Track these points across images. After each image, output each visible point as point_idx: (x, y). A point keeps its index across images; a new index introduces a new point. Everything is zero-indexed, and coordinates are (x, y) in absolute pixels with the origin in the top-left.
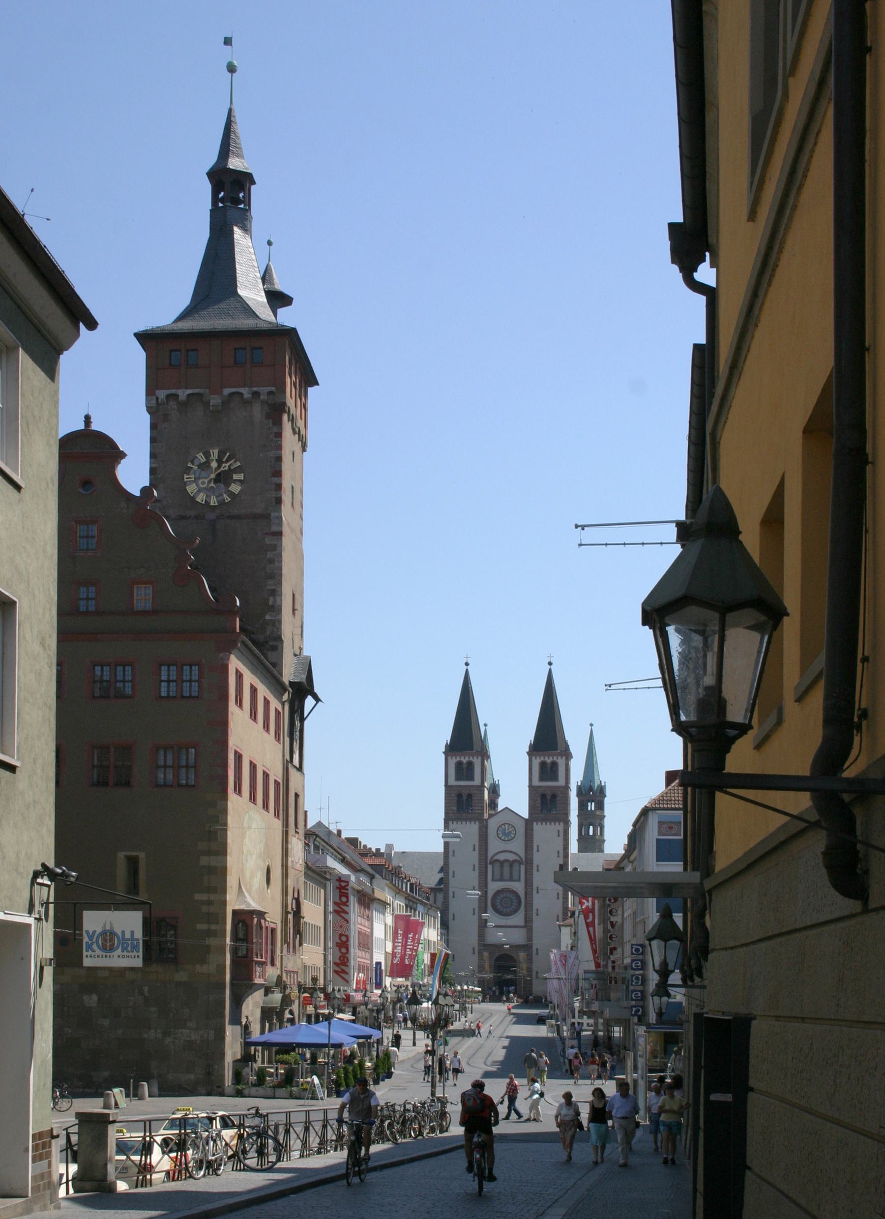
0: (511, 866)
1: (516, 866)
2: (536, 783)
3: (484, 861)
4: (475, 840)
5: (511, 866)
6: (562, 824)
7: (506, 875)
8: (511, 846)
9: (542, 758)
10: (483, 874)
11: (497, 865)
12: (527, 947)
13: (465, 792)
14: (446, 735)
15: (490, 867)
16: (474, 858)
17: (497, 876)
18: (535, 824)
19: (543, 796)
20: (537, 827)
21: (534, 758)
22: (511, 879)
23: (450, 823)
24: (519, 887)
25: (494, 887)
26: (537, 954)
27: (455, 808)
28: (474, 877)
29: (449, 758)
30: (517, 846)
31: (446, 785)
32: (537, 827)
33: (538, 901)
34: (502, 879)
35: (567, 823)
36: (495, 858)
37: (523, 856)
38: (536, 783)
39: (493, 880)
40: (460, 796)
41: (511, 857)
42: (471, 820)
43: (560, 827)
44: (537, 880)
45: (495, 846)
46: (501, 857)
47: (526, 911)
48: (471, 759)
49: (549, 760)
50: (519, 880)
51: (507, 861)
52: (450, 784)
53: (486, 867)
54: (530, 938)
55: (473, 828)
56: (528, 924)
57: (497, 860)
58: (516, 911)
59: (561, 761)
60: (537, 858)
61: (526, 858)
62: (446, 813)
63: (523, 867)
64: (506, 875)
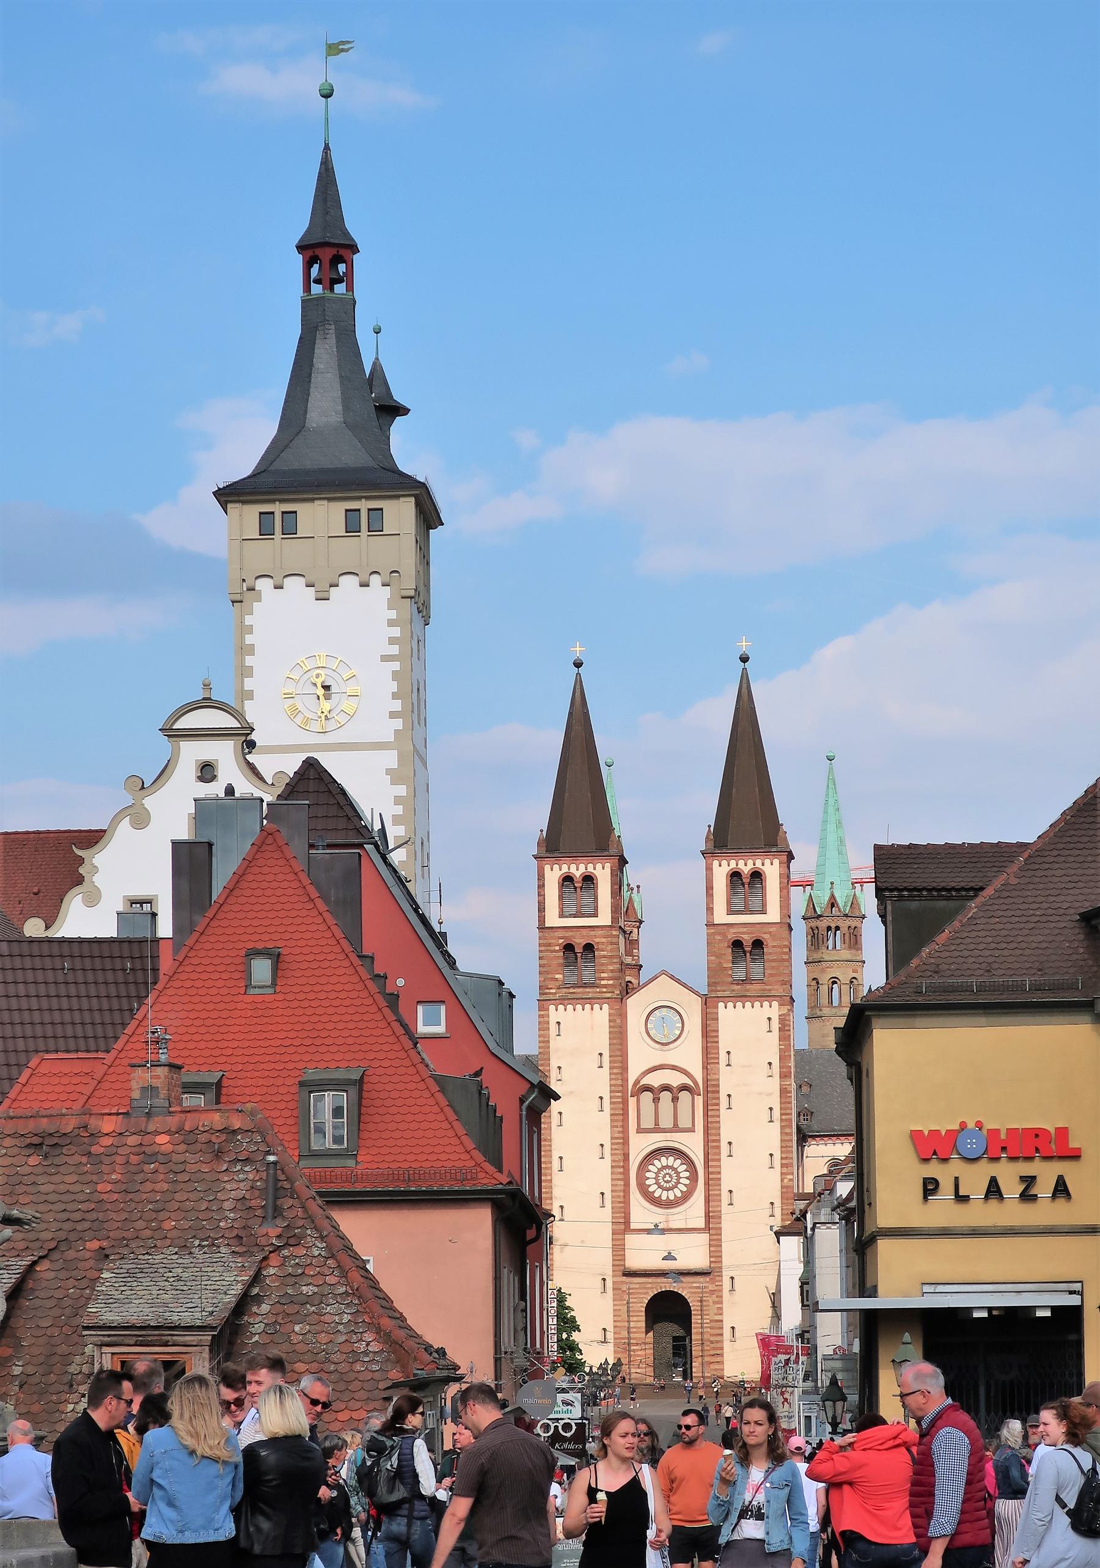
0: (675, 1099)
3: (624, 1093)
4: (602, 1041)
5: (675, 1099)
6: (775, 1004)
7: (666, 1122)
8: (671, 1056)
9: (733, 864)
10: (620, 1117)
13: (579, 941)
14: (537, 816)
15: (632, 1101)
16: (601, 1082)
17: (648, 1122)
18: (721, 1005)
20: (729, 1015)
21: (716, 863)
22: (676, 1128)
23: (552, 1008)
24: (693, 1144)
25: (640, 1145)
26: (732, 1290)
29: (547, 868)
30: (688, 1055)
31: (542, 927)
32: (729, 1015)
33: (730, 1174)
34: (657, 1129)
36: (645, 1081)
37: (699, 1076)
38: (721, 916)
39: (640, 1130)
40: (569, 948)
41: (675, 1079)
42: (591, 1001)
43: (773, 1010)
45: (641, 1056)
46: (655, 1080)
47: (707, 1200)
48: (590, 868)
49: (746, 867)
50: (692, 1130)
51: (666, 1088)
55: (601, 1015)
56: (712, 1223)
57: (648, 1088)
58: (686, 1196)
59: (772, 869)
60: (727, 1081)
61: (706, 1081)
63: (699, 1101)
64: (666, 1122)
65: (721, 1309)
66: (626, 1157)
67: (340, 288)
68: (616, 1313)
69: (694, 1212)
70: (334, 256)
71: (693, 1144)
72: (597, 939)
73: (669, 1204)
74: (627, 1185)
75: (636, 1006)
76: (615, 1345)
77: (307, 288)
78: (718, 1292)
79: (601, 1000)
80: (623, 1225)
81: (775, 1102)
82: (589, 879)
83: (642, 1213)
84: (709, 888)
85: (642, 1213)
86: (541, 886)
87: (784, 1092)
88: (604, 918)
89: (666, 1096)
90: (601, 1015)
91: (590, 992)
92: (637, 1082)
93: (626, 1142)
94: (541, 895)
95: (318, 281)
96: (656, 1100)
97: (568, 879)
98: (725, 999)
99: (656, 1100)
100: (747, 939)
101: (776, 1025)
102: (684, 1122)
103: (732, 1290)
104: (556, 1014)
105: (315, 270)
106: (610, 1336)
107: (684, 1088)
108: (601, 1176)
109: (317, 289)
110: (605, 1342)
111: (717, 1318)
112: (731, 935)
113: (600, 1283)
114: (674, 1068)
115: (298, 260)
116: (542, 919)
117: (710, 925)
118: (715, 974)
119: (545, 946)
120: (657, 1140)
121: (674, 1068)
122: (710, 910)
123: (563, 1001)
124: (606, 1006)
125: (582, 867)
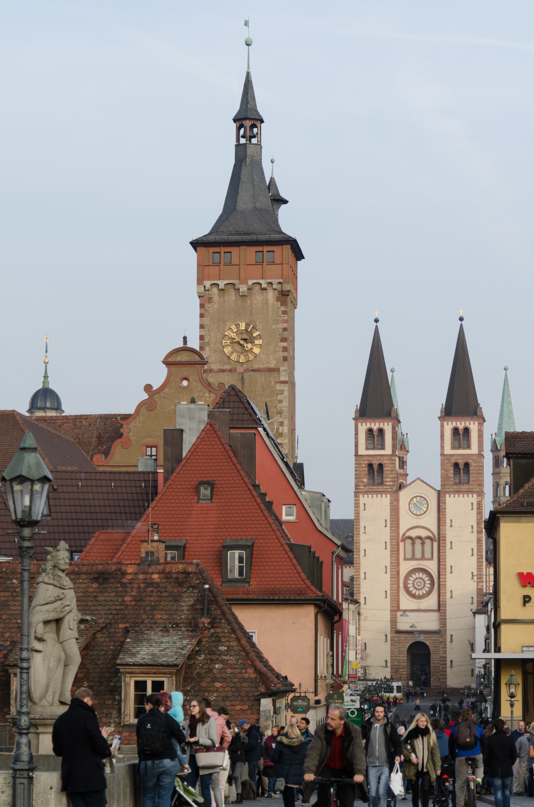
0: (423, 543)
1: (428, 542)
2: (448, 450)
3: (397, 540)
6: (475, 495)
7: (418, 555)
8: (422, 521)
11: (409, 542)
12: (440, 633)
13: (375, 462)
15: (401, 544)
16: (386, 534)
17: (409, 555)
18: (447, 496)
19: (456, 465)
20: (450, 500)
21: (445, 423)
22: (423, 558)
23: (361, 496)
24: (432, 566)
25: (405, 567)
26: (451, 641)
27: (365, 480)
28: (385, 558)
29: (359, 424)
30: (430, 521)
31: (356, 455)
32: (450, 500)
34: (413, 558)
35: (481, 494)
36: (408, 534)
38: (448, 450)
39: (405, 559)
40: (370, 466)
41: (424, 533)
42: (381, 493)
43: (474, 499)
44: (450, 559)
45: (406, 521)
46: (413, 533)
50: (432, 559)
51: (420, 538)
52: (360, 453)
53: (398, 545)
54: (443, 620)
55: (385, 500)
56: (441, 608)
57: (410, 538)
58: (429, 593)
59: (474, 427)
60: (450, 534)
61: (439, 534)
62: (356, 486)
63: (435, 544)
64: (418, 555)
65: (446, 651)
66: (398, 573)
67: (254, 141)
68: (392, 653)
69: (431, 601)
70: (252, 124)
71: (432, 566)
72: (385, 462)
73: (420, 597)
74: (398, 587)
75: (404, 496)
76: (392, 669)
77: (238, 140)
78: (444, 643)
79: (386, 492)
80: (395, 608)
81: (475, 546)
82: (381, 431)
83: (406, 602)
84: (442, 436)
85: (406, 602)
86: (356, 434)
87: (479, 541)
88: (388, 450)
89: (418, 542)
90: (385, 500)
91: (381, 488)
92: (404, 534)
93: (398, 565)
94: (356, 438)
95: (243, 137)
96: (413, 544)
97: (370, 430)
98: (449, 493)
99: (413, 544)
100: (461, 462)
101: (475, 507)
102: (428, 555)
103: (451, 641)
104: (363, 499)
105: (242, 131)
106: (389, 664)
107: (429, 538)
108: (385, 582)
109: (243, 141)
110: (386, 667)
111: (444, 655)
112: (453, 460)
113: (384, 637)
114: (423, 527)
115: (234, 126)
116: (356, 451)
117: (442, 455)
118: (444, 479)
119: (358, 465)
120: (414, 564)
121: (423, 527)
122: (442, 447)
123: (367, 492)
124: (388, 496)
125: (377, 424)
